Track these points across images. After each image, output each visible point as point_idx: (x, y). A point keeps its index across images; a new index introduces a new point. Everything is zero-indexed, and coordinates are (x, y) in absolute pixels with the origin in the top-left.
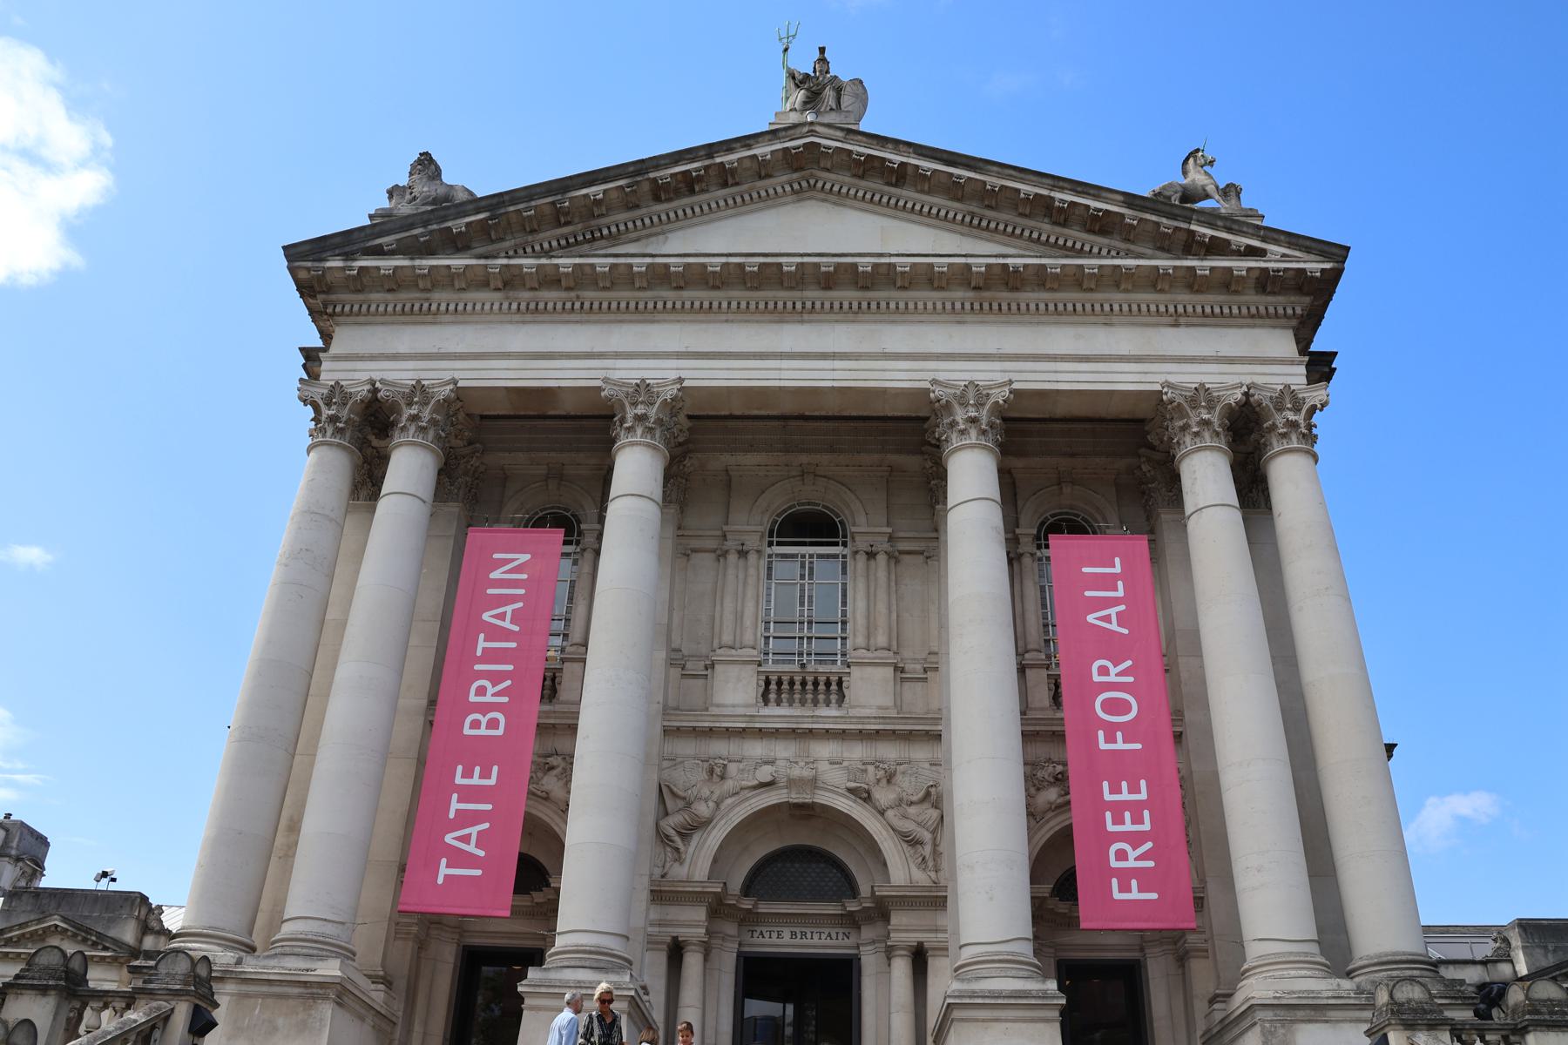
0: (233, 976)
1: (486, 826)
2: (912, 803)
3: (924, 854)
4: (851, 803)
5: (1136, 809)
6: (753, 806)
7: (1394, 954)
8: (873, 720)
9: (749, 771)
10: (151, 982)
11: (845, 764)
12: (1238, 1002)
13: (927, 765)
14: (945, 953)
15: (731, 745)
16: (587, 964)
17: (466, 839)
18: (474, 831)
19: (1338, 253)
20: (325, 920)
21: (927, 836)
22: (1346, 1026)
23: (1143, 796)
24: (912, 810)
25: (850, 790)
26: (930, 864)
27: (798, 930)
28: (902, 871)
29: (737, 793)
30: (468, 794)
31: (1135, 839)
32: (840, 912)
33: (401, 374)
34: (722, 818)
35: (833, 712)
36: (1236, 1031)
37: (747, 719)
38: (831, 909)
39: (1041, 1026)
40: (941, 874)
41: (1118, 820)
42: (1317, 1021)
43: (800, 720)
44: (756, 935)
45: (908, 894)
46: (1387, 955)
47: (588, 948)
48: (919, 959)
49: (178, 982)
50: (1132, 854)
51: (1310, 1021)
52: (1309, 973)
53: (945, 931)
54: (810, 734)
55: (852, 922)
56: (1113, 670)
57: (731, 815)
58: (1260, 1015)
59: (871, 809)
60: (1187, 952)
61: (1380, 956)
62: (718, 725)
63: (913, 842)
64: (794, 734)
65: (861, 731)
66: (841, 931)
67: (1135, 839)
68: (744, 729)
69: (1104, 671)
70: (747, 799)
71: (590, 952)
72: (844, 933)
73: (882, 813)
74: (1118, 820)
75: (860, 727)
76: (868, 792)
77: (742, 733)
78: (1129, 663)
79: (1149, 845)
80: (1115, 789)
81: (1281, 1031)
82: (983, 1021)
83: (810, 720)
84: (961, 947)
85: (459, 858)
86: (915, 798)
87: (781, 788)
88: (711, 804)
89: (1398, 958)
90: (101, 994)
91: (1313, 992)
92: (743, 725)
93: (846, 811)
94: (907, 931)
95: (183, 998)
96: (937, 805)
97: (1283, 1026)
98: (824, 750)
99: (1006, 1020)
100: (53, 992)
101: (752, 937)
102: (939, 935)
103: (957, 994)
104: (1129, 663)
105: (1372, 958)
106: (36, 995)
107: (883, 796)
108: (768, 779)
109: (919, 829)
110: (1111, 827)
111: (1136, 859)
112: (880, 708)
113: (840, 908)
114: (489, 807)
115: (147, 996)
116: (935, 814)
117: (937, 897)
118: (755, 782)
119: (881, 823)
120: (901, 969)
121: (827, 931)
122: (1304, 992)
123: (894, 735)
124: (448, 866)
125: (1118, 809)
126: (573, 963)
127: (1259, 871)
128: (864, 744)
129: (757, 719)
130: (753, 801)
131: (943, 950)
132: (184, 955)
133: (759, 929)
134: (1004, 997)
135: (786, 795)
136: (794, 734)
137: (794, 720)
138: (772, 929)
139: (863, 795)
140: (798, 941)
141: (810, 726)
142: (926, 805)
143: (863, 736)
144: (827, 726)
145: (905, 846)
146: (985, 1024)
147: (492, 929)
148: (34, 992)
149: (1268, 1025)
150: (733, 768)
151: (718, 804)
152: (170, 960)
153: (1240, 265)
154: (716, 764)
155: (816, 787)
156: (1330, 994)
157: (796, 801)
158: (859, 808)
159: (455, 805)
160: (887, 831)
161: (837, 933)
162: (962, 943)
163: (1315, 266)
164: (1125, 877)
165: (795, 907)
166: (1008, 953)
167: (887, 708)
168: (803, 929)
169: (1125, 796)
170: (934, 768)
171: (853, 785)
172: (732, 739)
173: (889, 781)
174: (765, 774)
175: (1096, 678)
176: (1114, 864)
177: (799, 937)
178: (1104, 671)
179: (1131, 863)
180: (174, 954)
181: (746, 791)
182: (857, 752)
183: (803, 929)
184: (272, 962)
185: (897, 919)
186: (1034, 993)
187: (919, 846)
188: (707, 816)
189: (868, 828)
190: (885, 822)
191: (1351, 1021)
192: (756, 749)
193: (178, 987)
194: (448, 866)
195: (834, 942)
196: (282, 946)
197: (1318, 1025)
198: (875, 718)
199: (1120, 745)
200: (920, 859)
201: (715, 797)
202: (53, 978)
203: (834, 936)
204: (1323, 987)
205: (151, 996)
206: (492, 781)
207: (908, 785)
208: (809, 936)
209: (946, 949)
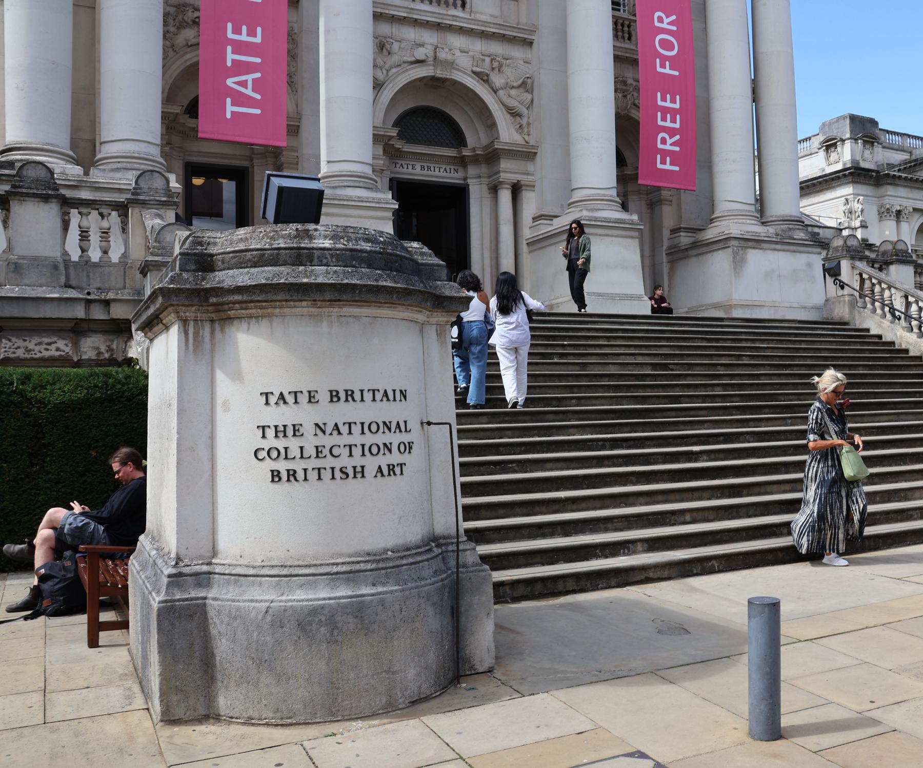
0: (88, 185)
1: (258, 75)
2: (513, 87)
3: (522, 123)
4: (475, 82)
5: (674, 112)
6: (411, 76)
7: (790, 216)
8: (492, 25)
9: (407, 49)
10: (138, 194)
11: (471, 53)
12: (711, 234)
13: (522, 62)
14: (532, 189)
15: (394, 29)
16: (362, 185)
17: (244, 84)
18: (249, 78)
20: (149, 142)
21: (525, 111)
22: (769, 252)
23: (677, 106)
24: (513, 92)
25: (474, 72)
26: (526, 130)
27: (425, 165)
28: (507, 133)
29: (400, 65)
30: (239, 47)
31: (672, 132)
32: (455, 155)
34: (390, 83)
35: (459, 13)
36: (705, 249)
37: (408, 10)
38: (450, 152)
39: (629, 240)
40: (531, 137)
41: (664, 119)
42: (757, 248)
43: (445, 17)
44: (398, 166)
45: (514, 149)
46: (787, 216)
47: (359, 174)
48: (516, 190)
49: (162, 195)
50: (669, 141)
51: (754, 248)
52: (755, 222)
53: (532, 175)
54: (450, 28)
55: (462, 162)
56: (666, 20)
57: (396, 81)
58: (733, 243)
59: (489, 89)
60: (661, 201)
61: (783, 216)
62: (387, 12)
63: (514, 113)
64: (438, 27)
65: (483, 32)
66: (453, 167)
67: (672, 132)
68: (405, 18)
69: (660, 20)
70: (407, 70)
71: (360, 177)
72: (455, 169)
73: (495, 91)
74: (664, 119)
75: (483, 28)
76: (488, 75)
77: (402, 21)
78: (674, 17)
79: (678, 137)
80: (664, 99)
81: (741, 252)
82: (600, 235)
83: (451, 18)
84: (572, 190)
85: (240, 99)
86: (515, 84)
87: (429, 65)
88: (385, 72)
89: (793, 218)
90: (90, 202)
91: (757, 233)
92: (405, 15)
93: (472, 87)
94: (511, 172)
95: (170, 207)
96: (530, 90)
97: (742, 250)
98: (457, 41)
99: (612, 236)
100: (54, 200)
101: (396, 167)
102: (529, 177)
103: (587, 218)
104: (674, 17)
105: (779, 217)
106: (38, 201)
107: (497, 80)
108: (422, 58)
109: (520, 106)
110: (660, 123)
111: (671, 145)
112: (492, 16)
113: (455, 152)
114: (258, 60)
115: (139, 205)
116: (529, 97)
117: (530, 152)
118: (413, 59)
119: (494, 98)
120: (505, 196)
121: (444, 167)
122: (753, 232)
123: (503, 38)
124: (232, 105)
125: (665, 111)
126: (352, 184)
127: (734, 162)
128: (483, 41)
129: (415, 12)
130: (411, 72)
131: (532, 187)
132: (158, 174)
133: (400, 162)
134: (613, 222)
135: (433, 71)
136: (438, 27)
137: (440, 16)
138: (408, 162)
139: (483, 77)
140: (425, 172)
141: (451, 23)
142: (521, 90)
143: (484, 35)
144: (462, 25)
145: (508, 116)
146: (602, 237)
147: (204, 150)
148: (36, 199)
149: (735, 248)
150: (396, 46)
151: (388, 71)
152: (147, 178)
154: (387, 42)
155: (454, 69)
156: (765, 235)
157: (440, 76)
158: (480, 86)
159: (230, 57)
160: (498, 105)
161: (450, 169)
162: (573, 188)
164: (664, 153)
165: (450, 152)
166: (604, 195)
167: (497, 17)
168: (429, 165)
169: (668, 104)
170: (526, 65)
171: (476, 69)
172: (394, 24)
173: (499, 70)
174: (420, 54)
175: (657, 24)
176: (660, 146)
177: (426, 169)
178: (660, 20)
179: (668, 147)
180: (150, 173)
181: (406, 65)
182: (478, 46)
183: (429, 165)
184: (118, 175)
185: (505, 164)
186: (628, 222)
187: (517, 117)
188: (382, 80)
189: (485, 101)
190: (497, 98)
191: (771, 250)
192: (410, 34)
193: (165, 199)
194: (232, 105)
195: (448, 175)
196: (119, 162)
197: (757, 250)
198: (494, 24)
199: (667, 71)
200: (519, 126)
201: (387, 66)
202: (49, 189)
203: (448, 171)
204: (754, 228)
205: (144, 206)
206: (258, 39)
207: (511, 75)
208: (432, 169)
209: (534, 186)
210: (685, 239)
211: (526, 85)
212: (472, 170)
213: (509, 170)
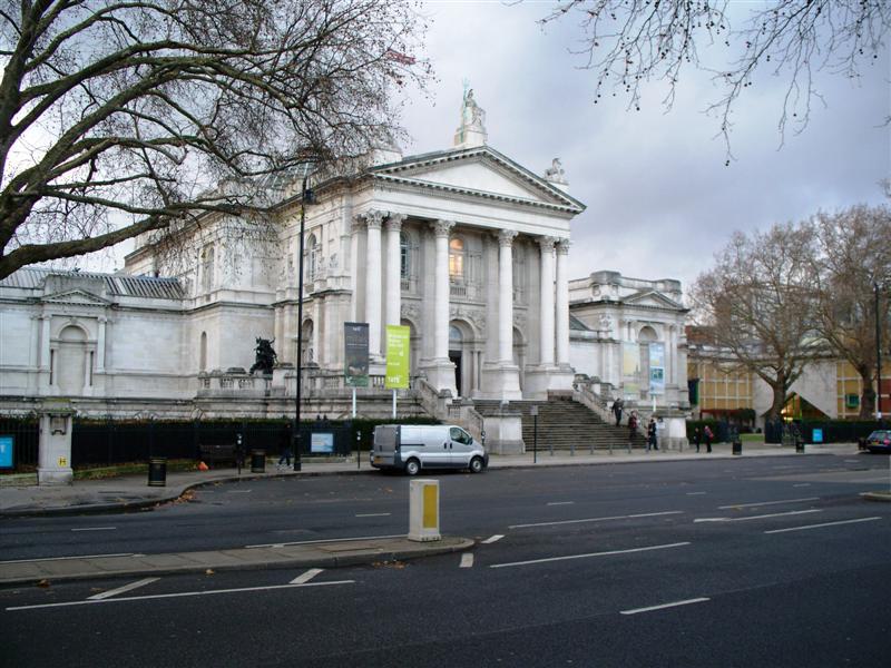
12: (539, 369)
19: (584, 207)
28: (478, 336)
33: (393, 209)
48: (479, 353)
55: (461, 343)
63: (479, 329)
98: (463, 306)
107: (475, 319)
120: (476, 355)
153: (566, 207)
163: (579, 209)
182: (468, 308)
185: (476, 345)
204: (555, 368)
210: (531, 369)
211: (484, 320)
212: (464, 346)
213: (477, 348)
